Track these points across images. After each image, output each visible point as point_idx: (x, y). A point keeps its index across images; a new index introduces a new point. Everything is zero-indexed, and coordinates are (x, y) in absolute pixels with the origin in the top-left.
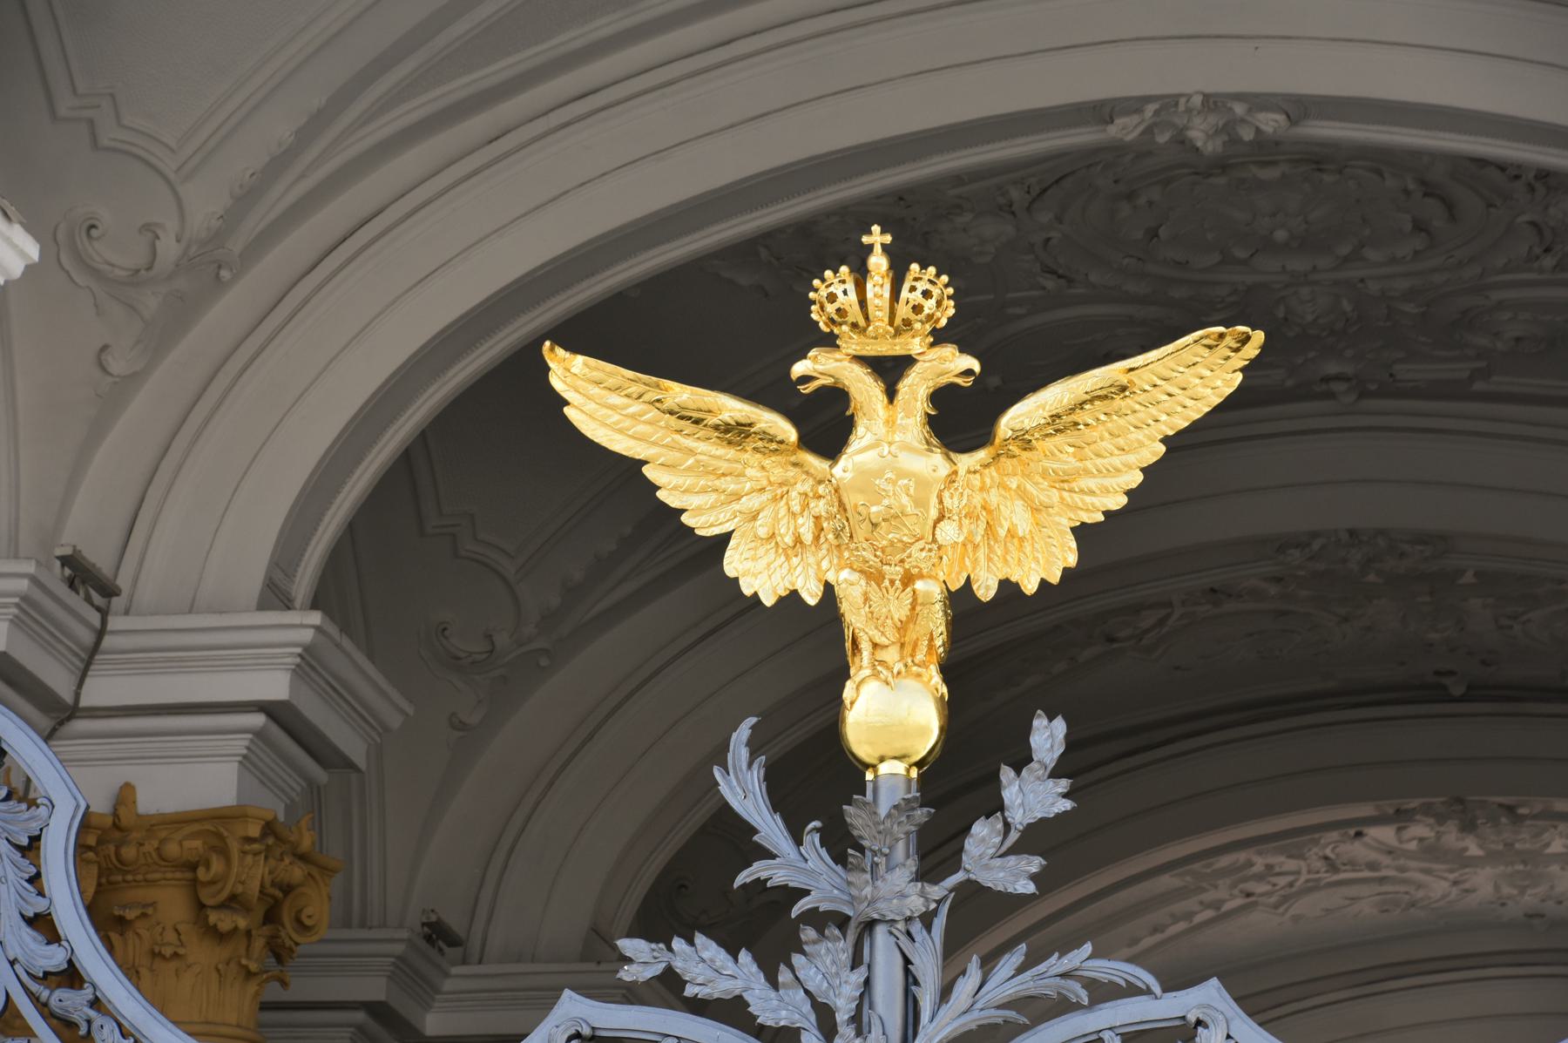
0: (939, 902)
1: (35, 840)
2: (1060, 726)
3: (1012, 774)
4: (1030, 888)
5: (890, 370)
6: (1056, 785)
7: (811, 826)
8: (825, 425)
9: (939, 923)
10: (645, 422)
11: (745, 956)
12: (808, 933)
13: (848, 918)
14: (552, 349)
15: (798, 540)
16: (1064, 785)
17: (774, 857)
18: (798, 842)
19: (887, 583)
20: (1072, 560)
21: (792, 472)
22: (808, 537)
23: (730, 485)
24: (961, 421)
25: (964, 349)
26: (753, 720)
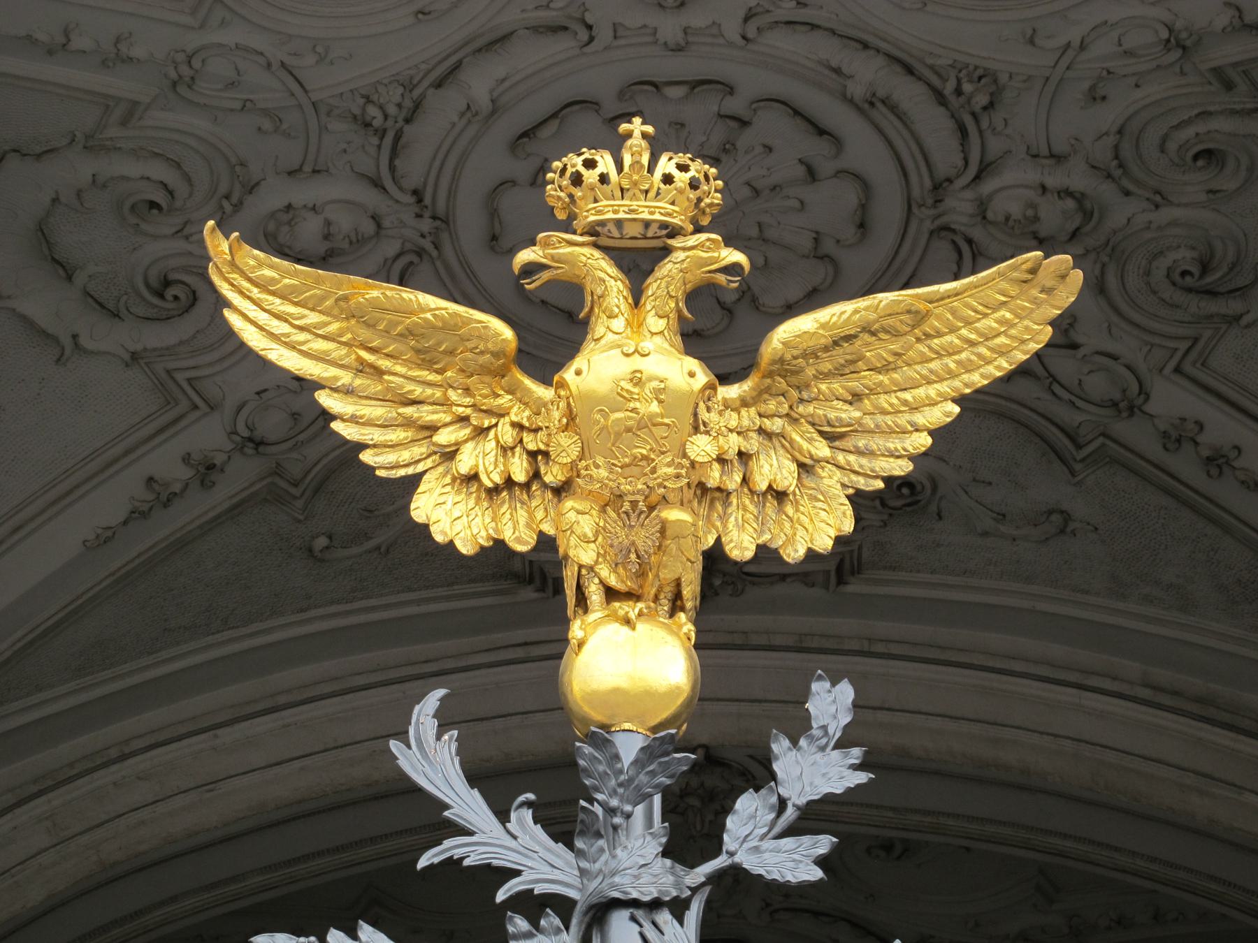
0: (694, 890)
2: (846, 691)
3: (786, 743)
5: (638, 259)
6: (846, 755)
7: (522, 798)
8: (552, 329)
9: (693, 915)
10: (324, 337)
13: (572, 903)
14: (213, 230)
15: (509, 483)
16: (856, 754)
17: (470, 833)
18: (503, 816)
19: (627, 506)
20: (848, 526)
21: (505, 400)
22: (520, 477)
23: (427, 414)
24: (720, 330)
25: (730, 241)
26: (441, 692)
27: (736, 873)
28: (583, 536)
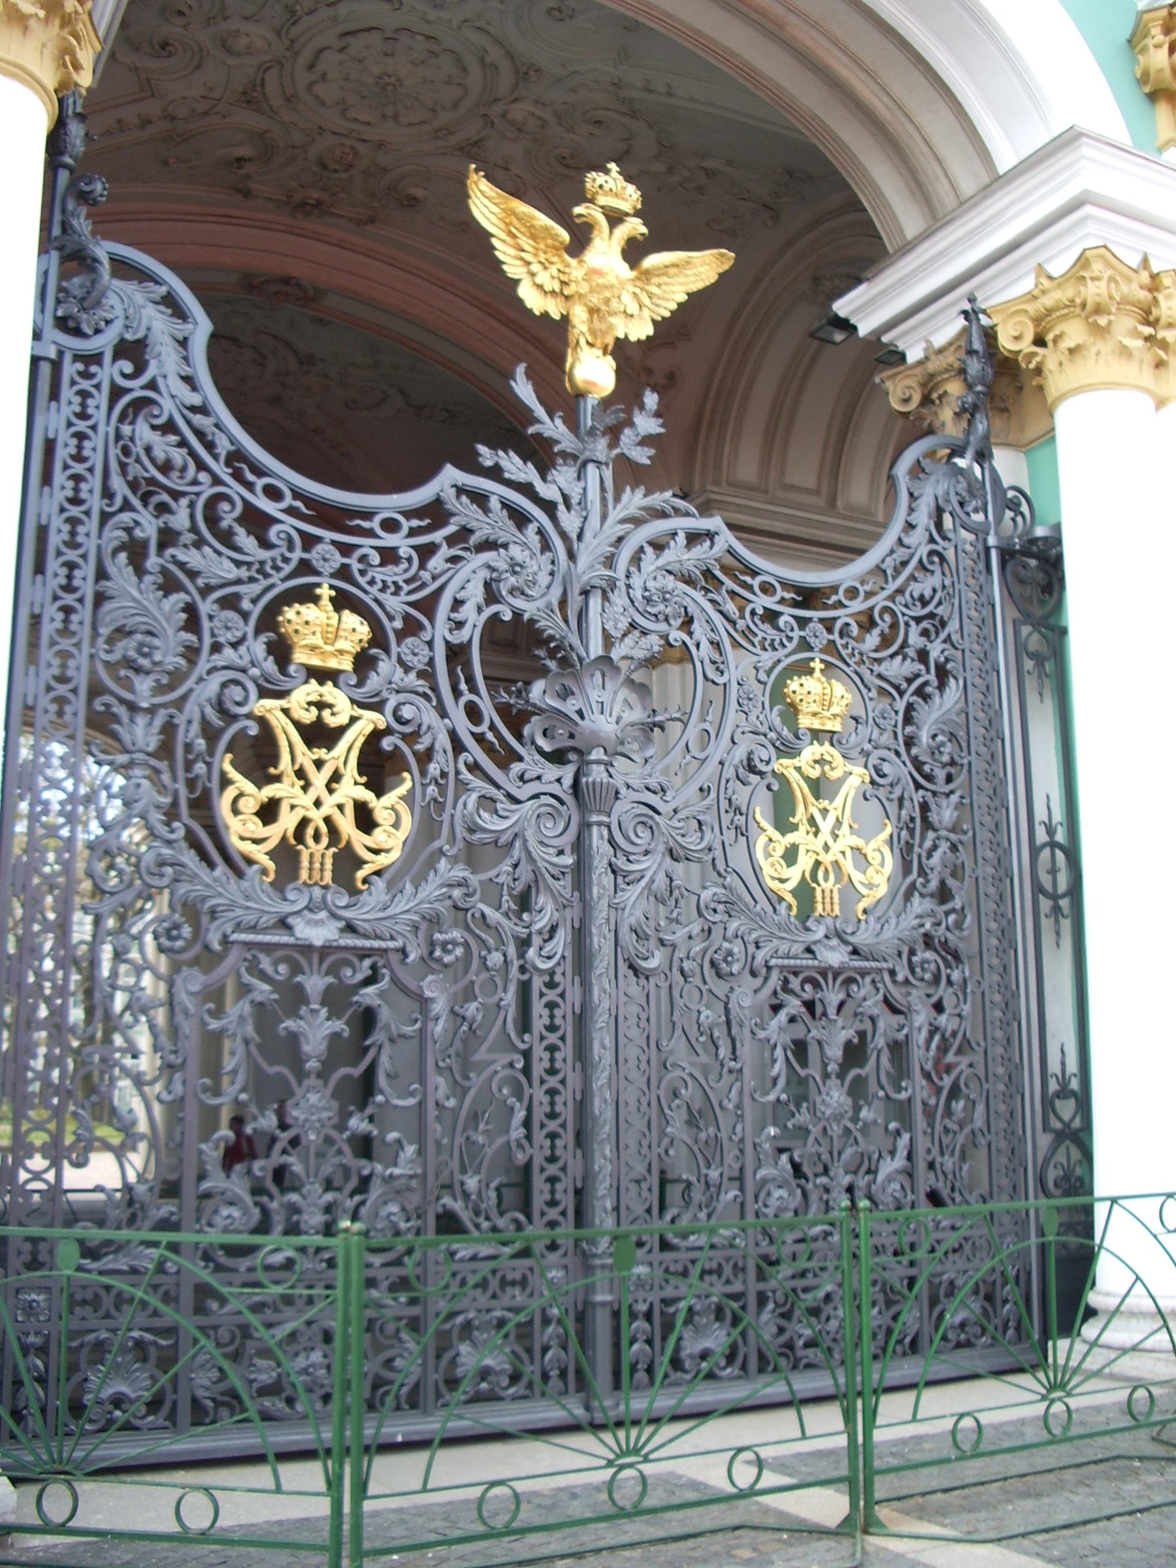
1: (186, 339)
4: (648, 462)
11: (530, 464)
12: (560, 461)
27: (623, 454)
28: (579, 315)
